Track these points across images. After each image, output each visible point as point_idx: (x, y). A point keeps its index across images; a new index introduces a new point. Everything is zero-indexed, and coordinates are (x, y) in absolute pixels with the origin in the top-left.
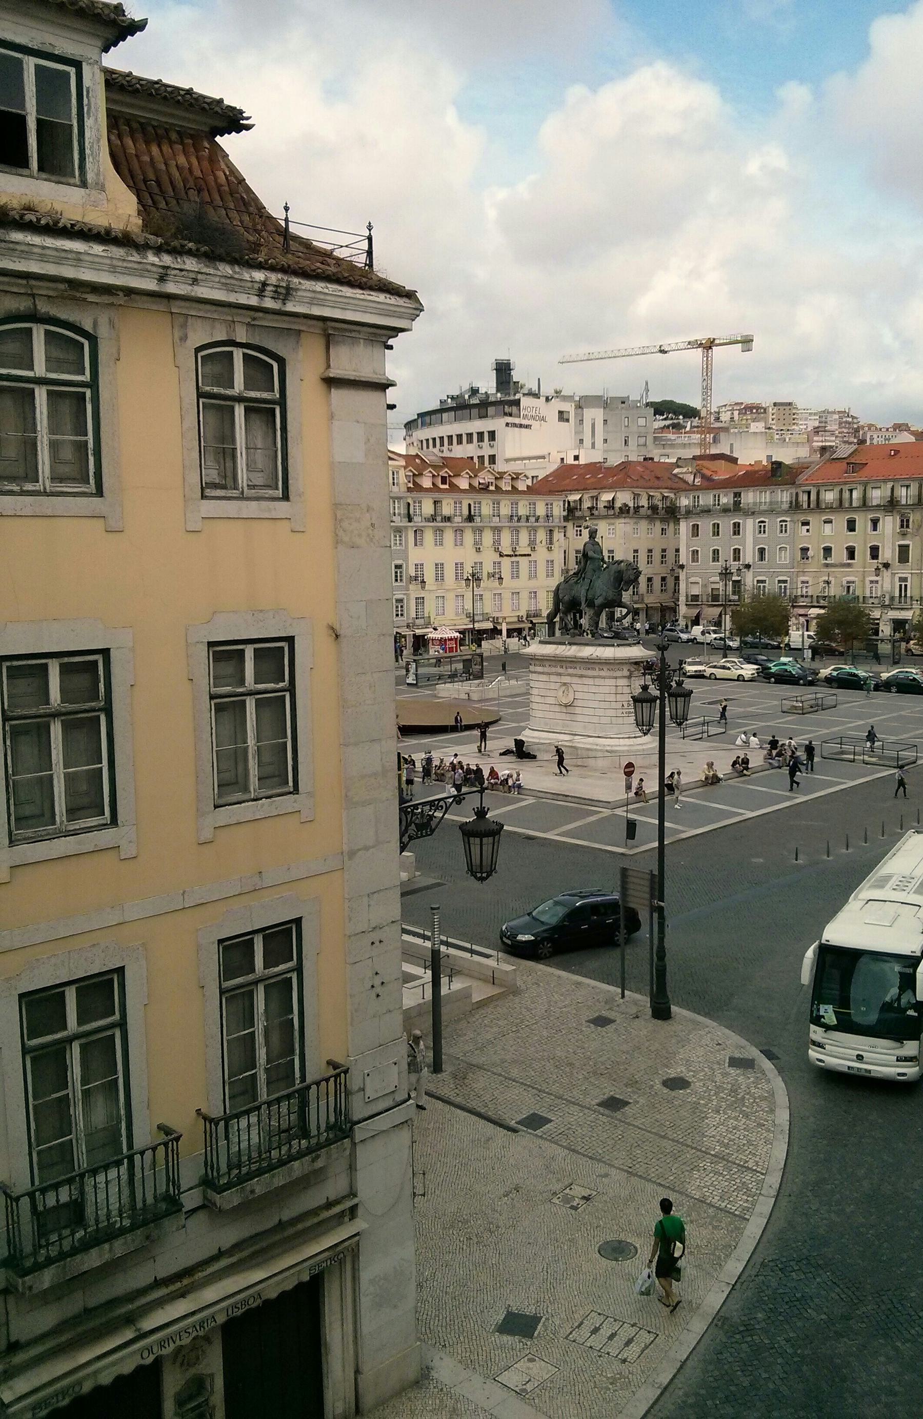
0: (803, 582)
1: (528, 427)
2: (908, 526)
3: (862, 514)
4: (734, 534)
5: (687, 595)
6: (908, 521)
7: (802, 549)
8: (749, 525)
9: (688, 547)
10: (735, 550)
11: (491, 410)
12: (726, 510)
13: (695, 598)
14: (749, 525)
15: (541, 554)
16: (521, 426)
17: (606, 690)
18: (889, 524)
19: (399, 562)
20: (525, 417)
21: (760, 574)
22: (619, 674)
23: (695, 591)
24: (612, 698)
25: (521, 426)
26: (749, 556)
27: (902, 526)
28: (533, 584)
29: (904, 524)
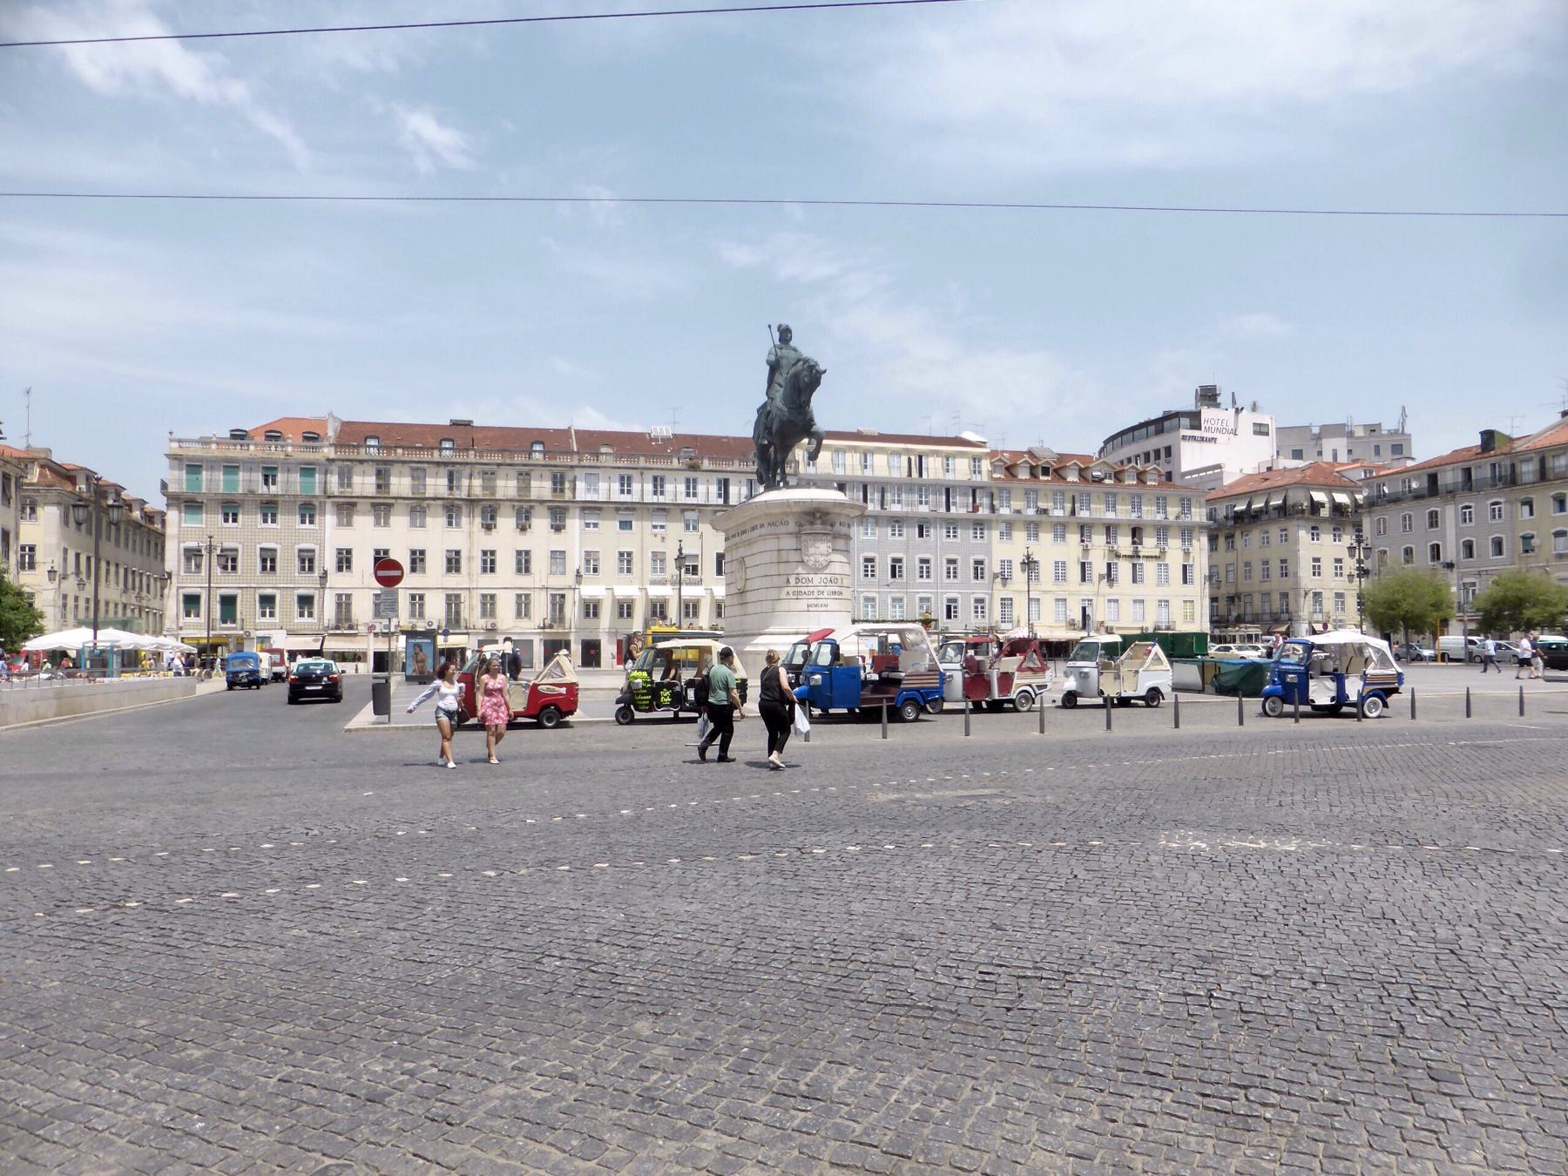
1: (1214, 440)
4: (1431, 526)
7: (1524, 538)
8: (1449, 513)
11: (1167, 424)
12: (1418, 497)
14: (1449, 513)
15: (1175, 557)
16: (1202, 439)
17: (766, 558)
19: (979, 557)
20: (1208, 429)
22: (783, 529)
24: (773, 570)
25: (1202, 439)
28: (1163, 592)
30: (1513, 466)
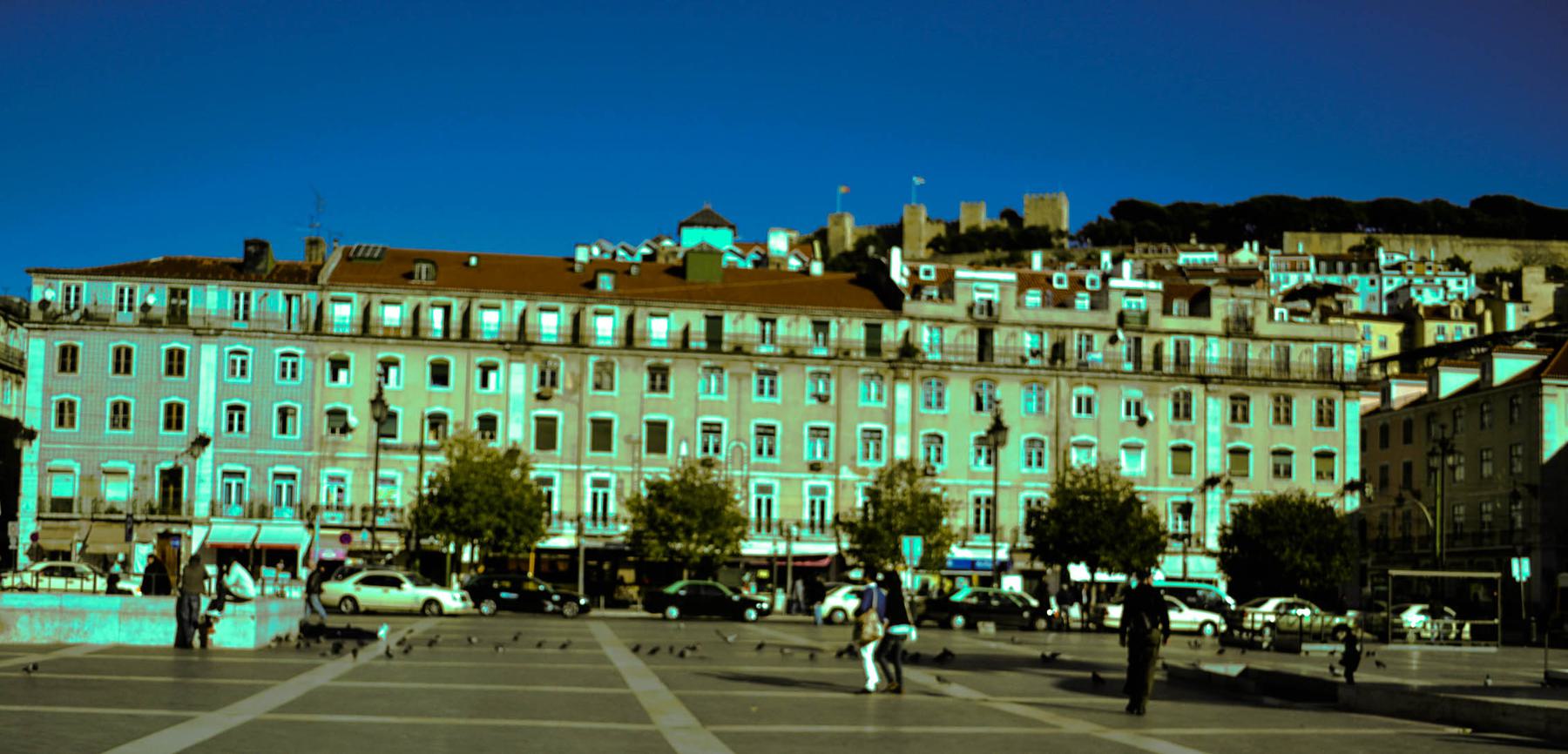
0: (332, 479)
2: (554, 384)
3: (462, 355)
4: (170, 371)
5: (40, 500)
6: (554, 374)
8: (208, 358)
9: (47, 392)
10: (169, 407)
12: (148, 321)
13: (63, 505)
14: (208, 358)
18: (517, 378)
21: (231, 458)
23: (63, 488)
26: (206, 416)
27: (542, 383)
29: (548, 379)
30: (320, 308)
